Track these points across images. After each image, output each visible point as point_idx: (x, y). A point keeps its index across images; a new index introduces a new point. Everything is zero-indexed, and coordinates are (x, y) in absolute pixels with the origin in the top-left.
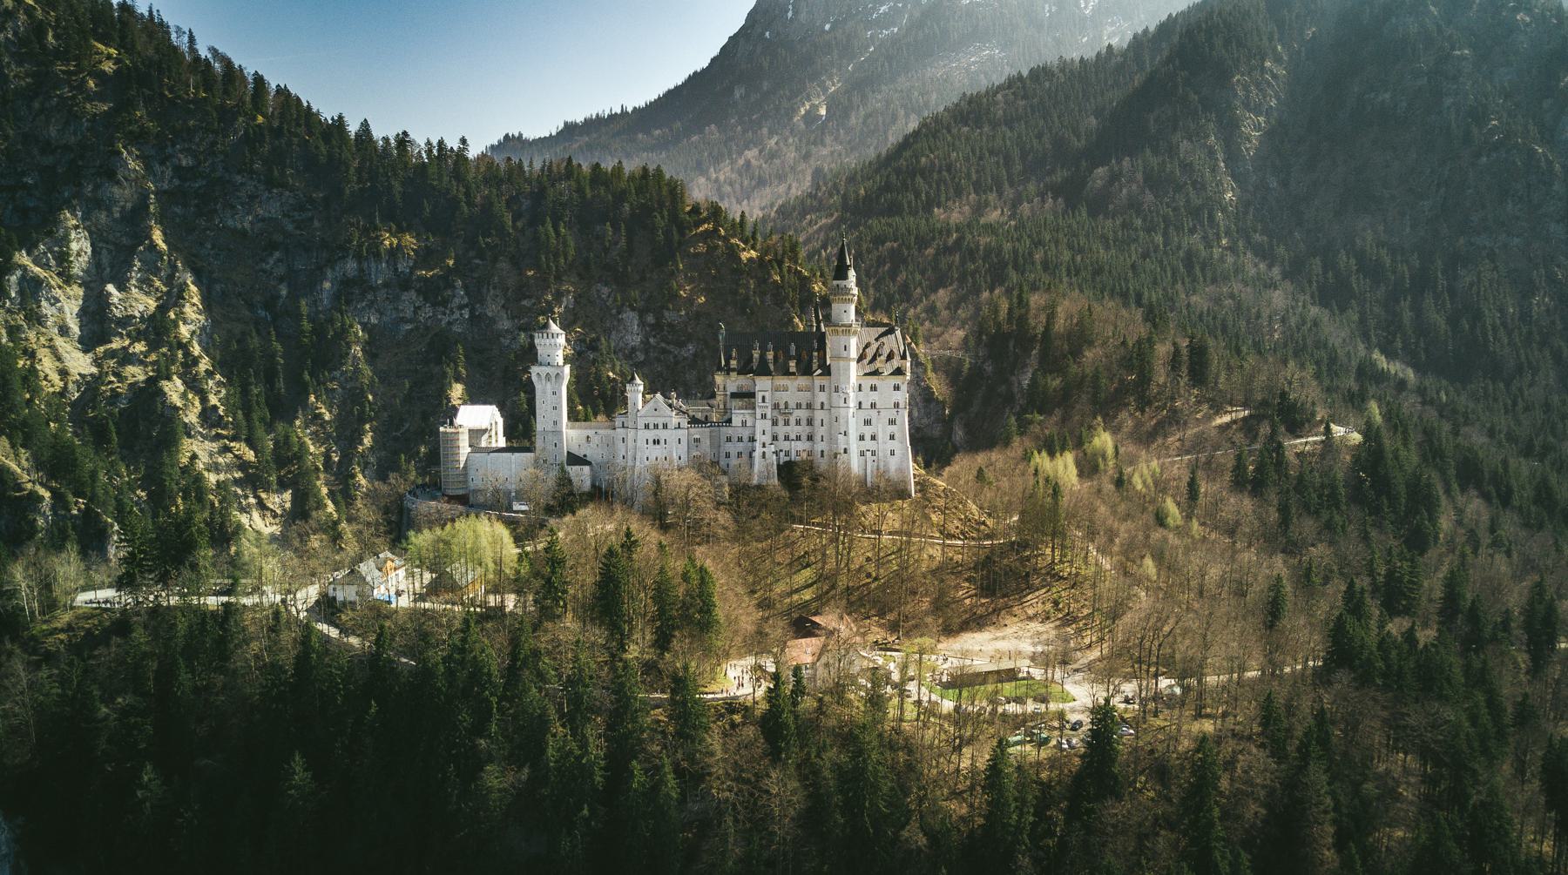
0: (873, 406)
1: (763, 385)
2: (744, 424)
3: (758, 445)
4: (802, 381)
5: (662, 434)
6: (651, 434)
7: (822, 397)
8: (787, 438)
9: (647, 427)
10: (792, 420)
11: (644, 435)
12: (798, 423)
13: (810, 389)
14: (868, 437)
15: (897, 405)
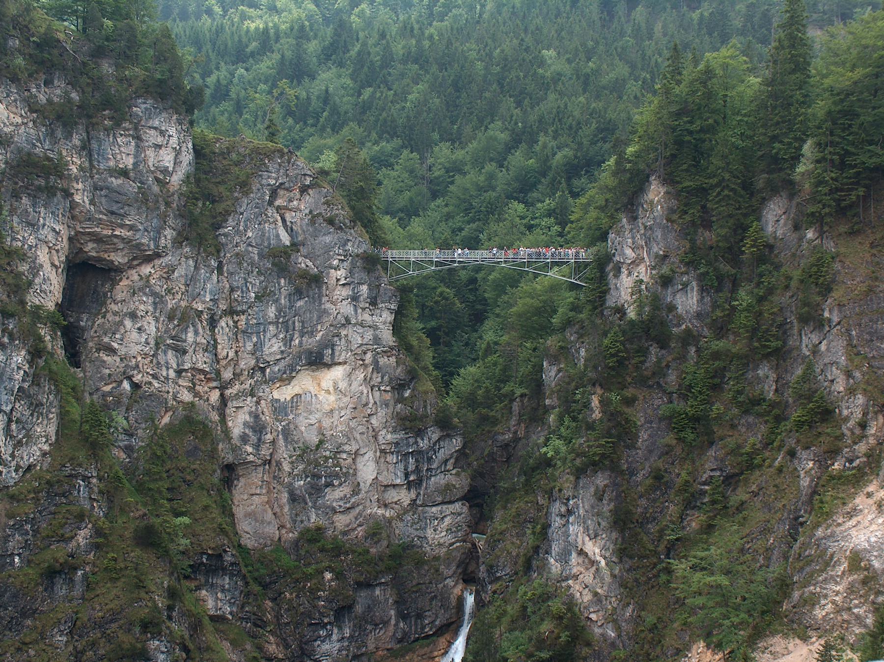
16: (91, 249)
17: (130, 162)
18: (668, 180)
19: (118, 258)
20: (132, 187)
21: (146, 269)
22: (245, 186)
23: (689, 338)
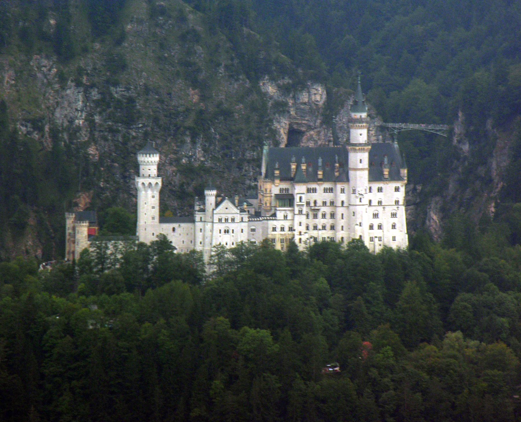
0: (380, 203)
1: (299, 189)
2: (286, 217)
3: (296, 233)
4: (327, 185)
5: (231, 226)
6: (223, 226)
7: (343, 197)
8: (315, 228)
9: (220, 220)
10: (320, 215)
11: (218, 226)
12: (324, 216)
13: (331, 190)
14: (376, 227)
15: (397, 202)
16: (295, 126)
17: (306, 100)
18: (462, 111)
19: (303, 129)
20: (307, 107)
21: (312, 132)
22: (343, 106)
23: (465, 158)
